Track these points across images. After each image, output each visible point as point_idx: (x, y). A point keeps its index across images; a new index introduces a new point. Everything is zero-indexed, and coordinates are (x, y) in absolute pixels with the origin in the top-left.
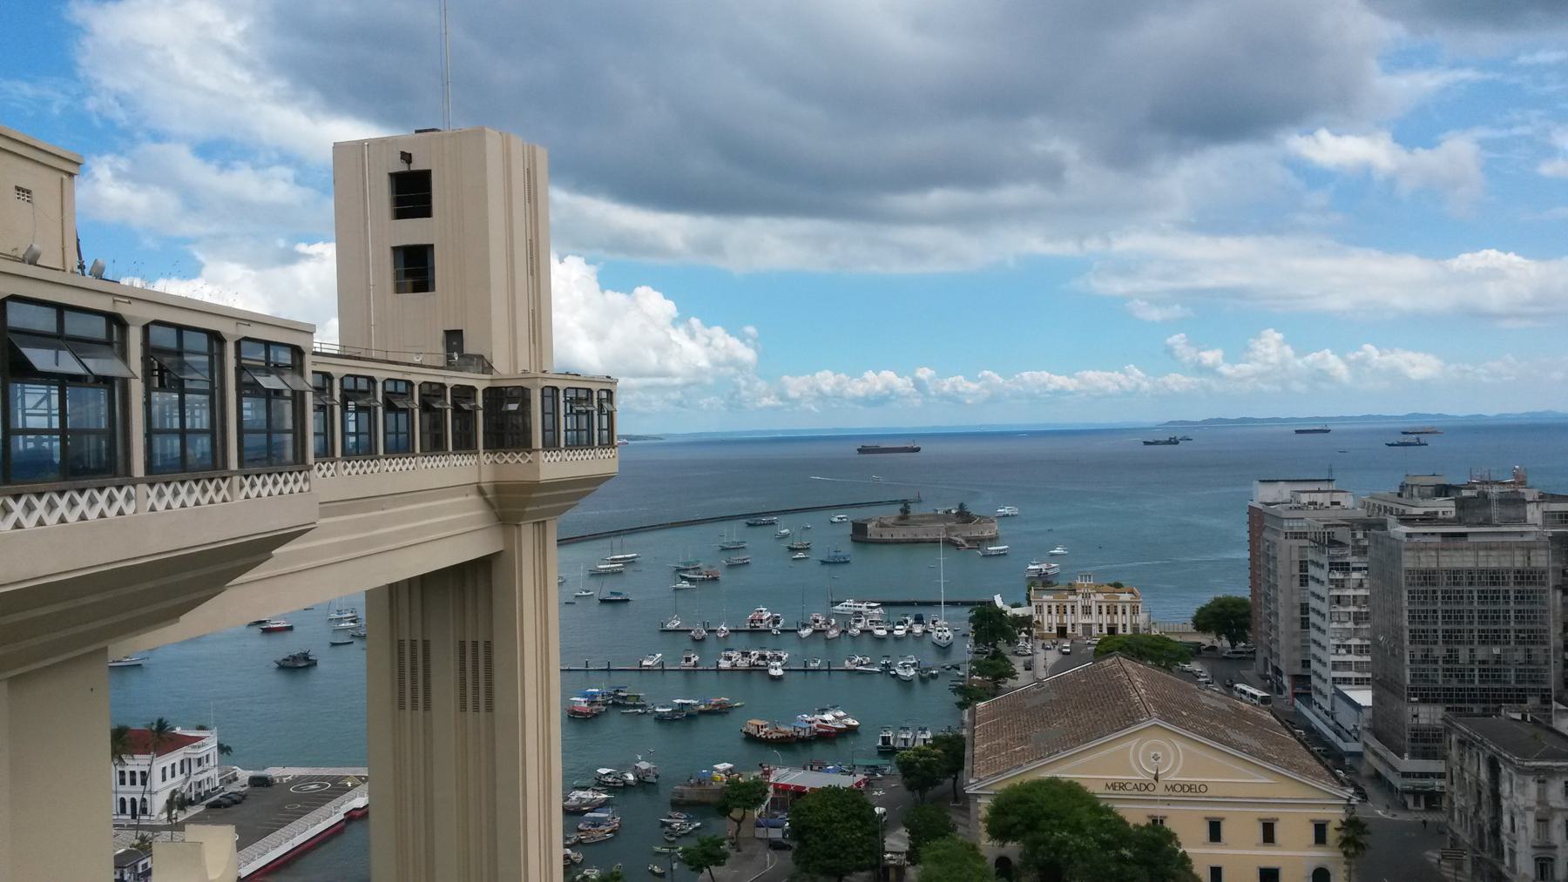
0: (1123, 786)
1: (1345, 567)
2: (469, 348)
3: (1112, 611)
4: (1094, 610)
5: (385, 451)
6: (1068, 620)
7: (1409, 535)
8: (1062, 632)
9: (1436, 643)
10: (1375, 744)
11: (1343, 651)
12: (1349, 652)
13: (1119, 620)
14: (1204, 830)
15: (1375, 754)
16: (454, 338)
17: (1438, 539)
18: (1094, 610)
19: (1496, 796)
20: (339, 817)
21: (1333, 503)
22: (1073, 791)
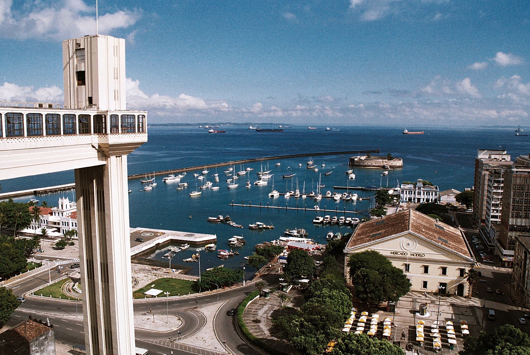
0: (397, 253)
1: (499, 182)
2: (94, 103)
3: (428, 193)
4: (422, 193)
5: (64, 134)
6: (412, 196)
7: (517, 172)
8: (410, 199)
9: (521, 210)
10: (498, 245)
11: (495, 212)
12: (497, 212)
13: (431, 197)
14: (441, 271)
15: (498, 247)
16: (90, 100)
17: (527, 174)
18: (422, 193)
19: (525, 263)
20: (153, 245)
21: (503, 159)
22: (374, 254)
